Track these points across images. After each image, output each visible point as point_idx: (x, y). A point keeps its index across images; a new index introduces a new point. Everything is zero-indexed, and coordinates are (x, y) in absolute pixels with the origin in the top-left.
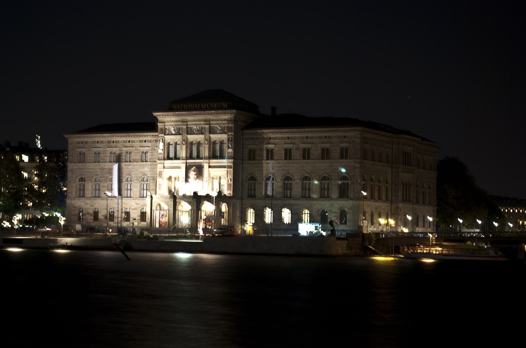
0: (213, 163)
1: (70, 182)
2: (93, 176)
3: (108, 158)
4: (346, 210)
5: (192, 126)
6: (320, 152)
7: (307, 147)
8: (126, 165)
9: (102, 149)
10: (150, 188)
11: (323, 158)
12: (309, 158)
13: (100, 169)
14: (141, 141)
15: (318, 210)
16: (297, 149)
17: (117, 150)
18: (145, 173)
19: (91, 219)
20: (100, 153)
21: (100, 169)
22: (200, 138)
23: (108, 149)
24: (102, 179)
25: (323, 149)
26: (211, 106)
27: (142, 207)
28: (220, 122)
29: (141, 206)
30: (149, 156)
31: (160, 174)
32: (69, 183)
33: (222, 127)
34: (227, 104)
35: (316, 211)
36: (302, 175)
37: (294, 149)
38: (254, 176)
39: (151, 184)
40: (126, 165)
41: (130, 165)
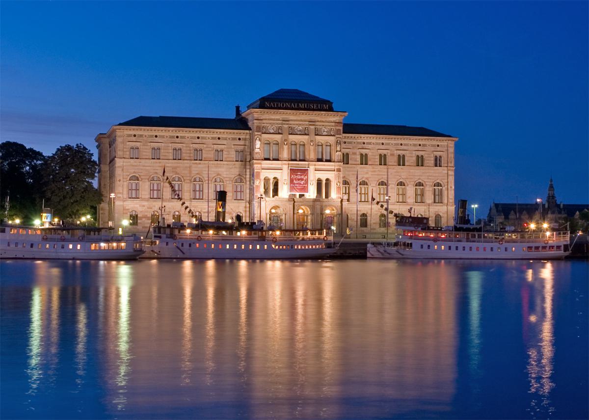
0: (319, 165)
1: (120, 181)
2: (151, 174)
4: (441, 214)
5: (294, 126)
6: (414, 159)
8: (196, 163)
9: (163, 144)
12: (404, 165)
16: (392, 155)
17: (183, 147)
19: (148, 223)
20: (160, 149)
22: (304, 139)
23: (170, 145)
25: (418, 156)
26: (310, 106)
28: (327, 124)
31: (259, 173)
32: (118, 182)
33: (329, 129)
36: (397, 181)
37: (389, 154)
38: (347, 180)
40: (196, 163)
41: (200, 164)
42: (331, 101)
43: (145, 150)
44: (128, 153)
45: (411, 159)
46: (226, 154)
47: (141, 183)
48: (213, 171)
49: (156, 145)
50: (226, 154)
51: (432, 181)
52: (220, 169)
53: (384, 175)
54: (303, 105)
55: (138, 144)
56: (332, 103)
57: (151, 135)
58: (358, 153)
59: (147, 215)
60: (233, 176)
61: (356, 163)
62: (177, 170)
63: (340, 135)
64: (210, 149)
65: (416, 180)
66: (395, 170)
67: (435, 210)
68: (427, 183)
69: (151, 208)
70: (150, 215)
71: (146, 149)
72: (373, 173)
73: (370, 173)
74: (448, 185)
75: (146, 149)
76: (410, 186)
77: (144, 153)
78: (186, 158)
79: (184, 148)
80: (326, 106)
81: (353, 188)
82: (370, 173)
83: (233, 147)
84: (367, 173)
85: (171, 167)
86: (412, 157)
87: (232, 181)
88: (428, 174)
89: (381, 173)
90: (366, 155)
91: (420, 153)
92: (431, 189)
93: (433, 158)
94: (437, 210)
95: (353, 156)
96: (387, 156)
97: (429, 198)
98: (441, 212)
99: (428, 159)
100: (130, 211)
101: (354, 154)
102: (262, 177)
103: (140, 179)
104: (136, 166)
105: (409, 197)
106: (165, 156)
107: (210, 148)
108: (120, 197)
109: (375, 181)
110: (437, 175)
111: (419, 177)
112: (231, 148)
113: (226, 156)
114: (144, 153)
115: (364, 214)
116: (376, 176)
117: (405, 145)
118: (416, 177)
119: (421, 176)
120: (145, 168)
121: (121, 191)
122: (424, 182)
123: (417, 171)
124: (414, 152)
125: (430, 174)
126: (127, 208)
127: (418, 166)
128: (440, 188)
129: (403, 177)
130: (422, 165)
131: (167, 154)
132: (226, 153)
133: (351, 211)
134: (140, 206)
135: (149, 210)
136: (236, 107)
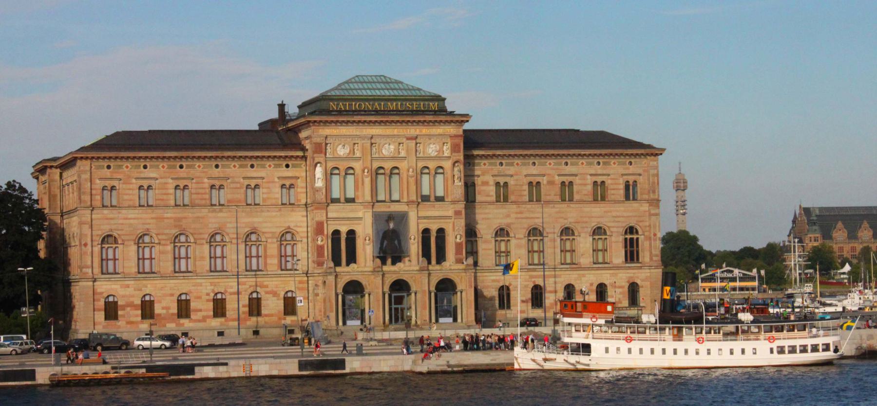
2: (139, 232)
3: (172, 197)
4: (639, 282)
6: (590, 188)
7: (567, 180)
10: (268, 254)
11: (595, 200)
12: (571, 200)
13: (152, 218)
14: (241, 166)
15: (592, 285)
18: (256, 225)
19: (137, 316)
21: (152, 218)
24: (160, 237)
25: (595, 183)
27: (252, 289)
29: (250, 286)
30: (263, 193)
34: (438, 105)
35: (589, 285)
37: (545, 182)
39: (268, 245)
40: (214, 211)
41: (221, 211)
42: (443, 96)
43: (127, 192)
44: (98, 197)
45: (583, 188)
46: (266, 193)
47: (121, 247)
48: (244, 223)
49: (145, 184)
50: (266, 193)
51: (620, 224)
52: (256, 220)
53: (538, 218)
54: (395, 103)
55: (115, 183)
56: (444, 99)
57: (136, 165)
58: (492, 182)
59: (133, 302)
60: (279, 230)
61: (489, 199)
62: (181, 224)
63: (459, 151)
64: (238, 185)
65: (593, 224)
66: (557, 210)
67: (628, 275)
68: (612, 229)
69: (141, 290)
70: (138, 302)
71: (130, 189)
72: (519, 216)
73: (513, 216)
74: (650, 231)
75: (130, 189)
76: (583, 235)
77: (126, 197)
78: (197, 202)
79: (194, 186)
80: (433, 105)
81: (486, 242)
82: (513, 216)
83: (276, 180)
84: (508, 216)
85: (171, 218)
86: (585, 185)
87: (277, 238)
88: (614, 214)
89: (532, 215)
90: (506, 184)
91: (599, 179)
92: (621, 239)
93: (622, 186)
94: (632, 275)
95: (484, 188)
96: (542, 186)
97: (618, 255)
98: (638, 277)
99: (612, 187)
100: (105, 295)
101: (485, 183)
102: (329, 229)
103: (120, 242)
104: (111, 219)
105: (582, 255)
106: (162, 200)
107: (237, 183)
108: (87, 273)
109: (524, 228)
110: (631, 214)
111: (599, 220)
112: (274, 182)
113: (265, 196)
114: (126, 197)
115: (502, 287)
116: (524, 220)
117: (572, 164)
118: (593, 219)
119: (602, 217)
120: (127, 221)
121: (89, 263)
122: (607, 227)
123: (594, 210)
124: (589, 177)
125: (618, 214)
126: (99, 290)
127: (597, 200)
128: (635, 237)
129: (570, 220)
130: (603, 198)
131: (165, 197)
132: (265, 190)
133: (483, 281)
134: (121, 287)
135: (137, 292)
136: (279, 105)
